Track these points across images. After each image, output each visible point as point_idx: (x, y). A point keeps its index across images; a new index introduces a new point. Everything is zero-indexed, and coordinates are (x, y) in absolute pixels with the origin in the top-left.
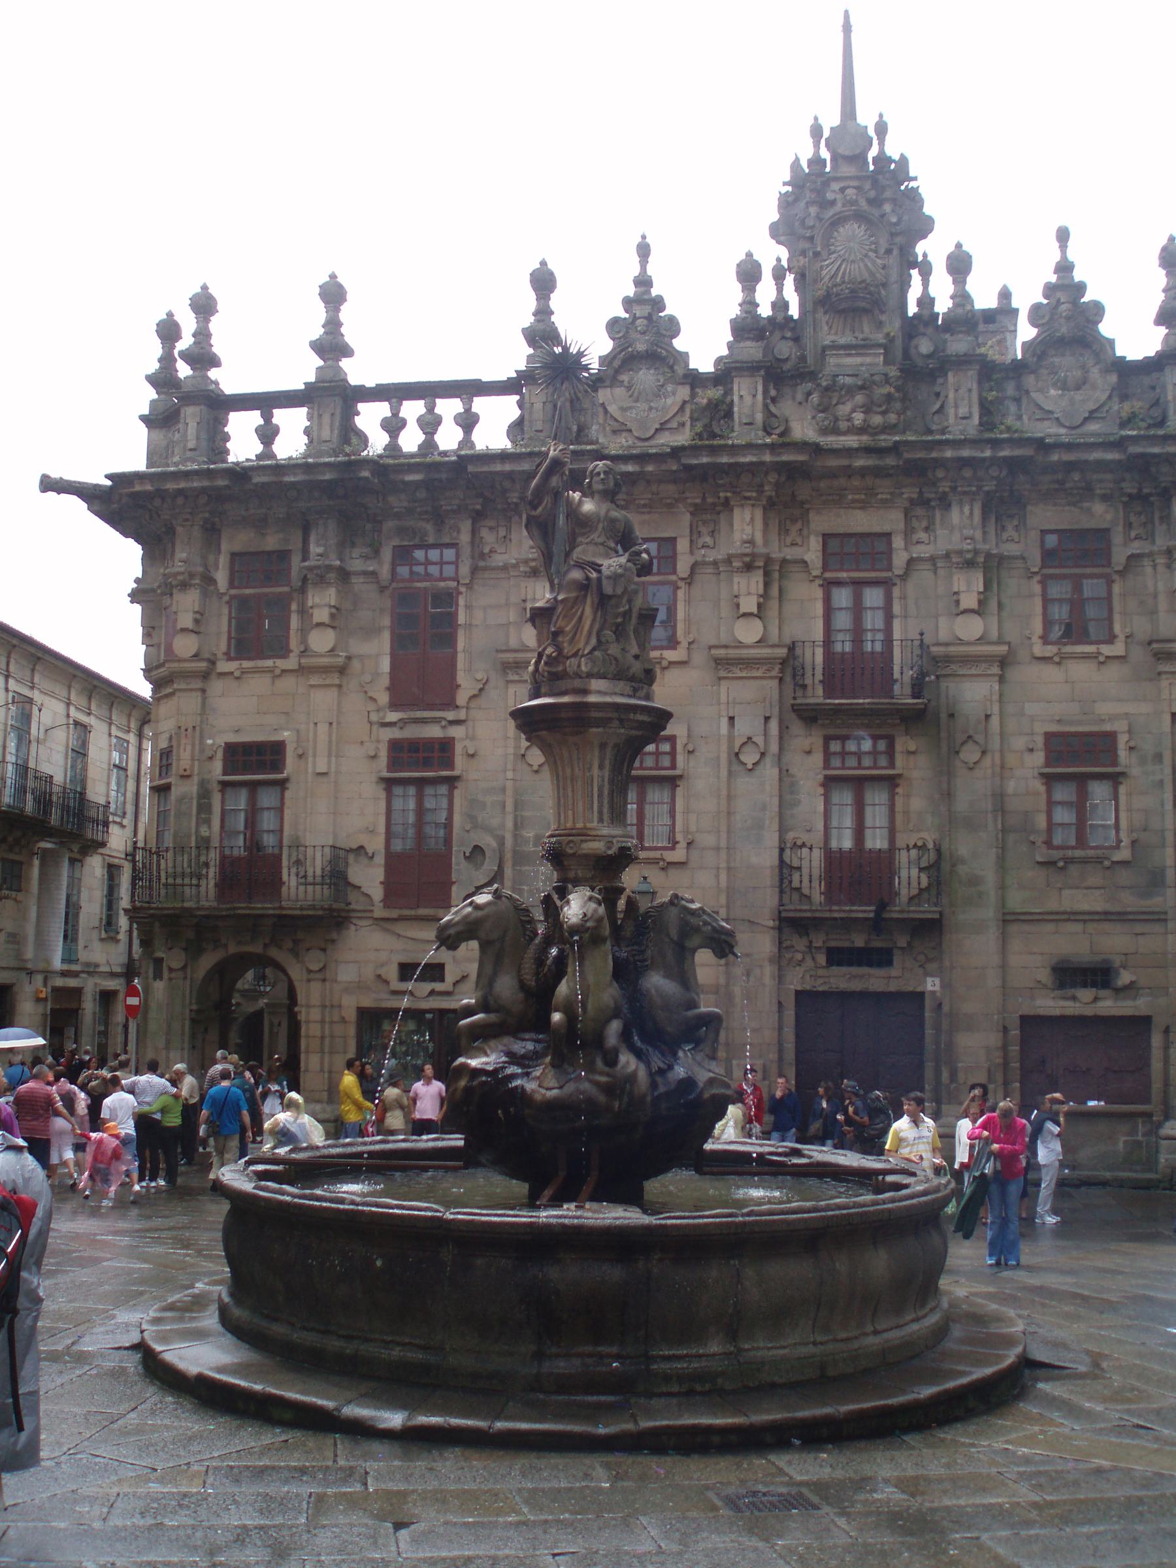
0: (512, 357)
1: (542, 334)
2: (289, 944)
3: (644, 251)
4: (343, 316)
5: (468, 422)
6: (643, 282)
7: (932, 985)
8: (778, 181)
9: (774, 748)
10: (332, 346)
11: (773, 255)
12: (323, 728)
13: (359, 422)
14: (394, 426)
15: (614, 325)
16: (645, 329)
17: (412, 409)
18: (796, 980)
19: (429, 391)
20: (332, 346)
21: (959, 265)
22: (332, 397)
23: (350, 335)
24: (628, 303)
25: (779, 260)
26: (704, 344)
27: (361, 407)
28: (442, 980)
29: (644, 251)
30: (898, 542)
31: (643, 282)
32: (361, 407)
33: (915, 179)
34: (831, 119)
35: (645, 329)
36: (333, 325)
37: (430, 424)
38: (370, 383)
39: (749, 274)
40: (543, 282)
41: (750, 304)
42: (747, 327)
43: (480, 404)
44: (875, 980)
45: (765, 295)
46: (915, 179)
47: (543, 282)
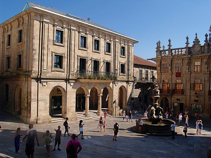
0: (185, 46)
1: (187, 43)
3: (196, 34)
5: (181, 51)
6: (196, 37)
10: (170, 46)
12: (170, 79)
14: (175, 52)
16: (197, 41)
17: (177, 51)
19: (178, 49)
20: (170, 46)
23: (171, 44)
24: (195, 40)
25: (210, 33)
26: (202, 43)
27: (173, 51)
29: (196, 34)
31: (196, 37)
32: (173, 51)
35: (197, 41)
37: (178, 52)
38: (173, 49)
39: (206, 36)
40: (187, 38)
41: (206, 39)
42: (206, 41)
43: (183, 50)
45: (208, 37)
47: (187, 38)
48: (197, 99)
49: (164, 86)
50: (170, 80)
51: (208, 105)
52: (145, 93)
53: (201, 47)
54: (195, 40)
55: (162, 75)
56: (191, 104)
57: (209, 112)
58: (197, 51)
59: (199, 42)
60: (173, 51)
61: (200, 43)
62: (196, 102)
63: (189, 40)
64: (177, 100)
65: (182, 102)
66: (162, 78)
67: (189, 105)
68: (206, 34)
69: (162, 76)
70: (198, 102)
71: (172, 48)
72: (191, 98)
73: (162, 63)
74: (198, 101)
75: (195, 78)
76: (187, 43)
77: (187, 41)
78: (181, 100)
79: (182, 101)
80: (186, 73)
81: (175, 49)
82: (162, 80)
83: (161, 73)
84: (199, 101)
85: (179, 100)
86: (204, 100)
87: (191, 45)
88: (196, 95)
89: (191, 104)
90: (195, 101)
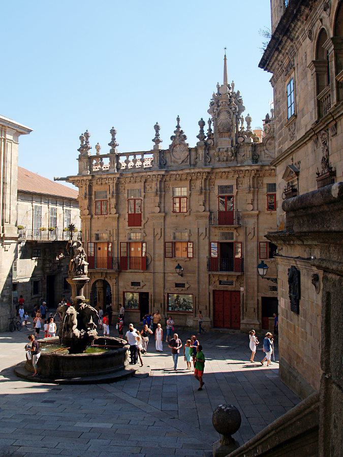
0: (150, 146)
1: (157, 141)
2: (109, 277)
3: (178, 119)
4: (116, 137)
5: (142, 160)
6: (178, 127)
7: (242, 289)
8: (208, 99)
9: (208, 235)
10: (113, 144)
11: (207, 117)
13: (120, 161)
14: (127, 162)
15: (172, 138)
16: (179, 137)
17: (131, 158)
18: (212, 288)
19: (134, 154)
21: (249, 120)
22: (114, 157)
23: (117, 141)
24: (175, 132)
25: (209, 119)
26: (192, 142)
27: (121, 157)
28: (140, 285)
29: (178, 119)
30: (235, 187)
31: (178, 127)
32: (121, 157)
33: (241, 97)
34: (221, 83)
35: (179, 137)
36: (114, 139)
37: (135, 161)
39: (202, 124)
40: (157, 128)
41: (202, 131)
42: (201, 136)
43: (146, 156)
44: (230, 288)
45: (206, 128)
46: (241, 97)
47: (157, 128)
48: (180, 280)
49: (100, 249)
50: (115, 235)
51: (208, 294)
52: (48, 271)
53: (190, 150)
54: (175, 132)
55: (93, 221)
56: (168, 294)
57: (209, 310)
58: (180, 162)
59: (185, 137)
60: (122, 159)
61: (186, 142)
62: (180, 289)
63: (160, 132)
64: (133, 284)
65: (144, 290)
66: (93, 228)
67: (162, 298)
68: (202, 119)
69: (93, 224)
70: (183, 289)
71: (118, 150)
72: (166, 277)
73: (94, 190)
74: (183, 285)
75: (174, 227)
76: (157, 141)
77: (157, 135)
78: (142, 284)
79: (144, 287)
80: (154, 214)
81: (127, 154)
82: (94, 235)
83: (92, 216)
84: (187, 286)
85: (138, 284)
86: (199, 283)
87: (165, 145)
88: (178, 270)
89: (168, 294)
90: (177, 285)
